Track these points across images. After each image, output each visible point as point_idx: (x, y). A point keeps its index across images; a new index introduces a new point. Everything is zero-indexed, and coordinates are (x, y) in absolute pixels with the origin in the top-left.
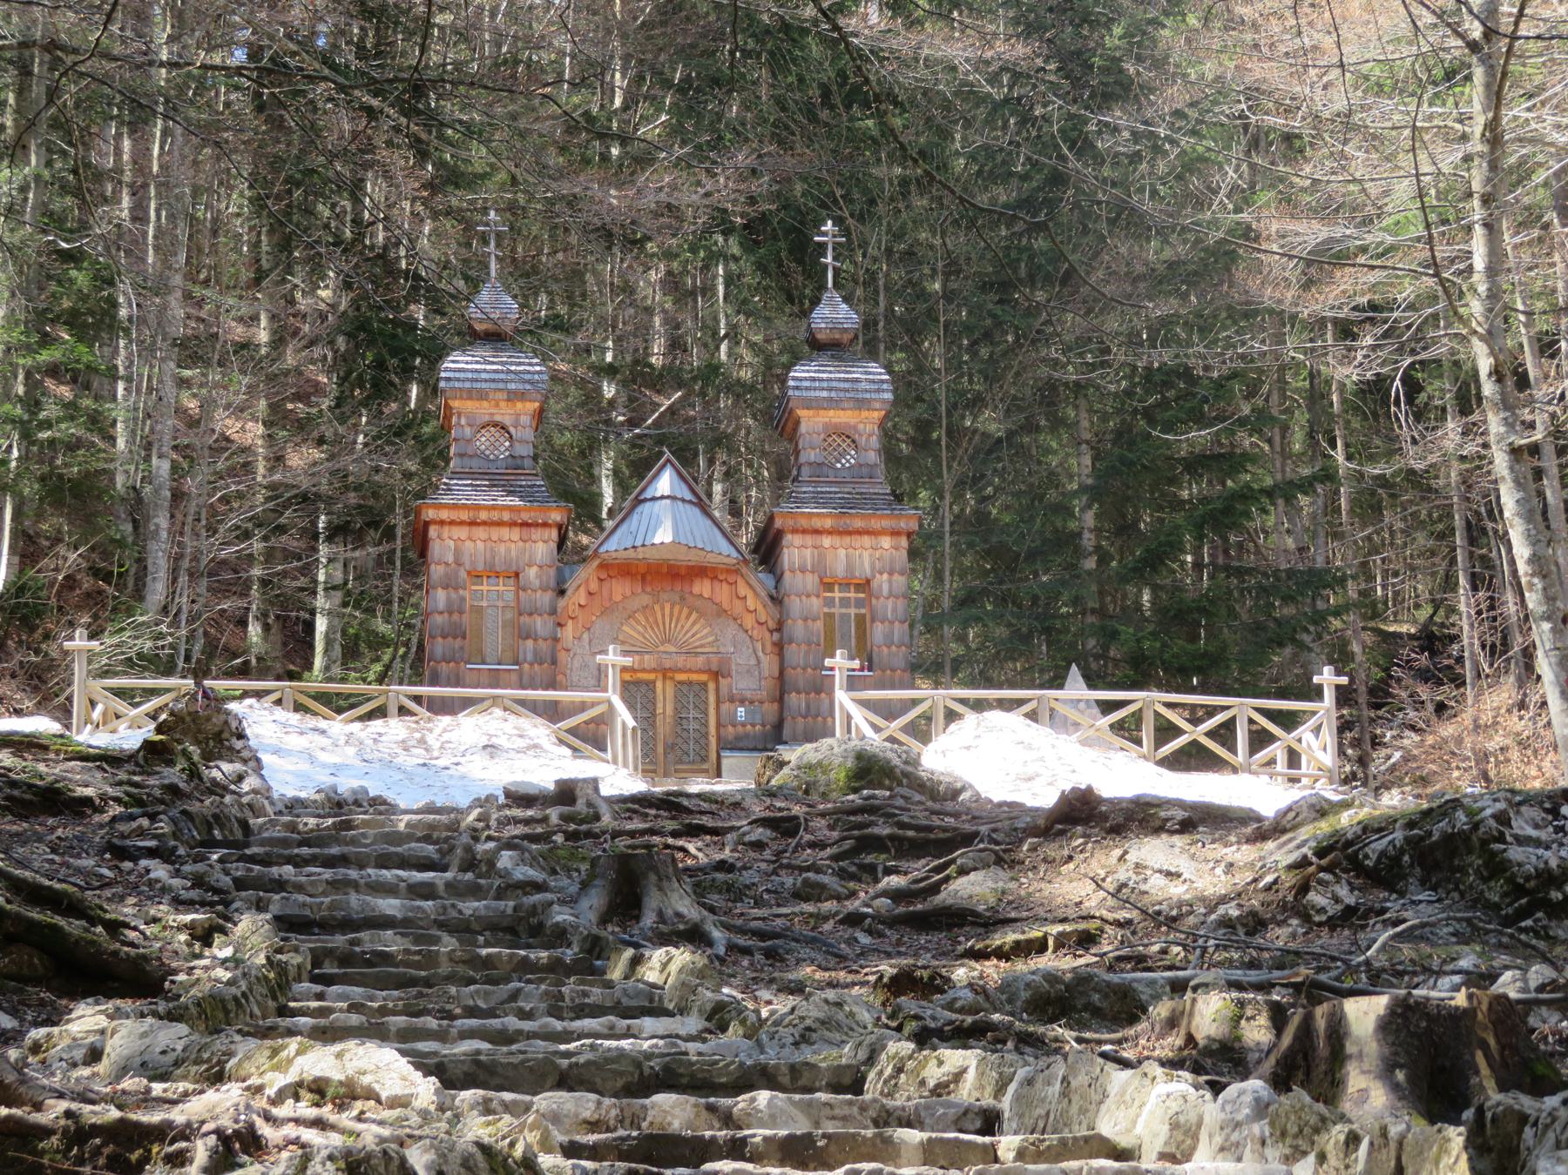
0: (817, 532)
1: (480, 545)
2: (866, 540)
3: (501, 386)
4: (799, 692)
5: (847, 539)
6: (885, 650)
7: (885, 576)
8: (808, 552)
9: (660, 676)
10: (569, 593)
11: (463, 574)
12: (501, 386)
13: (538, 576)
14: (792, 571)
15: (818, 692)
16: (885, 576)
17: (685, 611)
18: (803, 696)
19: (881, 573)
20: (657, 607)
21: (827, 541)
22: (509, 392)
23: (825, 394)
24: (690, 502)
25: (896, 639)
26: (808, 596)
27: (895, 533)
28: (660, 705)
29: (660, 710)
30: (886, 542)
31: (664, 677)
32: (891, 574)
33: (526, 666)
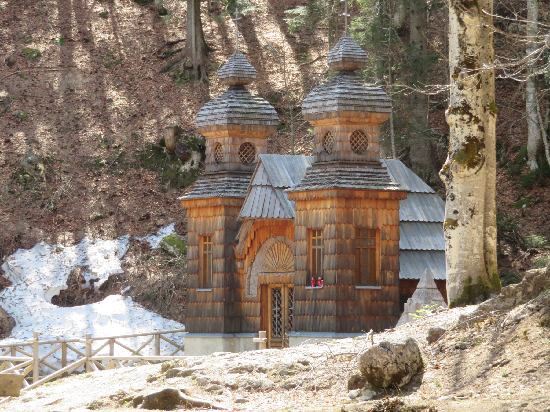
0: (305, 201)
1: (202, 218)
2: (322, 204)
3: (212, 123)
4: (299, 301)
5: (315, 204)
6: (328, 271)
7: (329, 225)
8: (303, 213)
9: (282, 284)
10: (240, 241)
11: (197, 237)
12: (212, 123)
13: (219, 237)
14: (298, 226)
15: (305, 300)
16: (329, 225)
17: (285, 246)
18: (300, 302)
19: (327, 224)
20: (276, 245)
21: (309, 206)
22: (218, 126)
23: (315, 111)
24: (266, 186)
25: (331, 266)
26: (303, 240)
27: (332, 198)
28: (283, 302)
29: (282, 306)
30: (329, 204)
31: (284, 286)
32: (331, 224)
33: (215, 289)
